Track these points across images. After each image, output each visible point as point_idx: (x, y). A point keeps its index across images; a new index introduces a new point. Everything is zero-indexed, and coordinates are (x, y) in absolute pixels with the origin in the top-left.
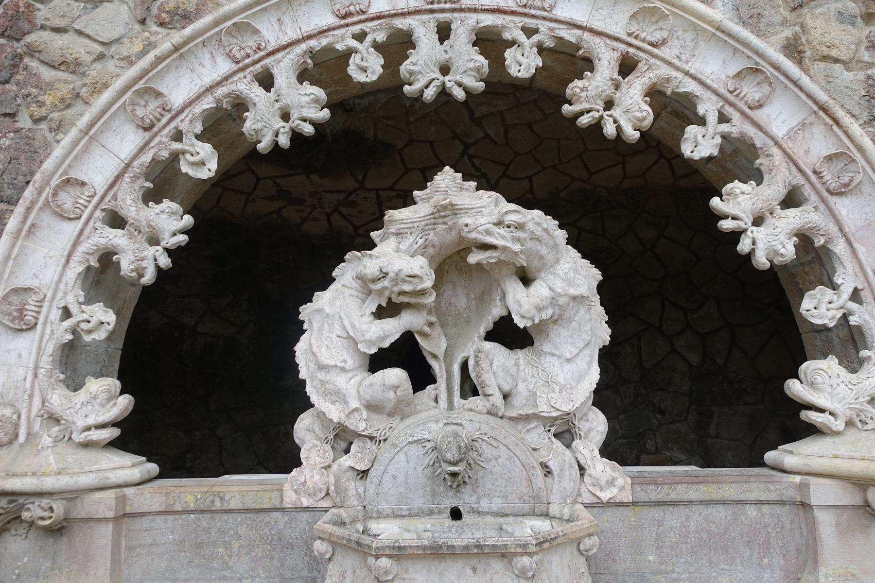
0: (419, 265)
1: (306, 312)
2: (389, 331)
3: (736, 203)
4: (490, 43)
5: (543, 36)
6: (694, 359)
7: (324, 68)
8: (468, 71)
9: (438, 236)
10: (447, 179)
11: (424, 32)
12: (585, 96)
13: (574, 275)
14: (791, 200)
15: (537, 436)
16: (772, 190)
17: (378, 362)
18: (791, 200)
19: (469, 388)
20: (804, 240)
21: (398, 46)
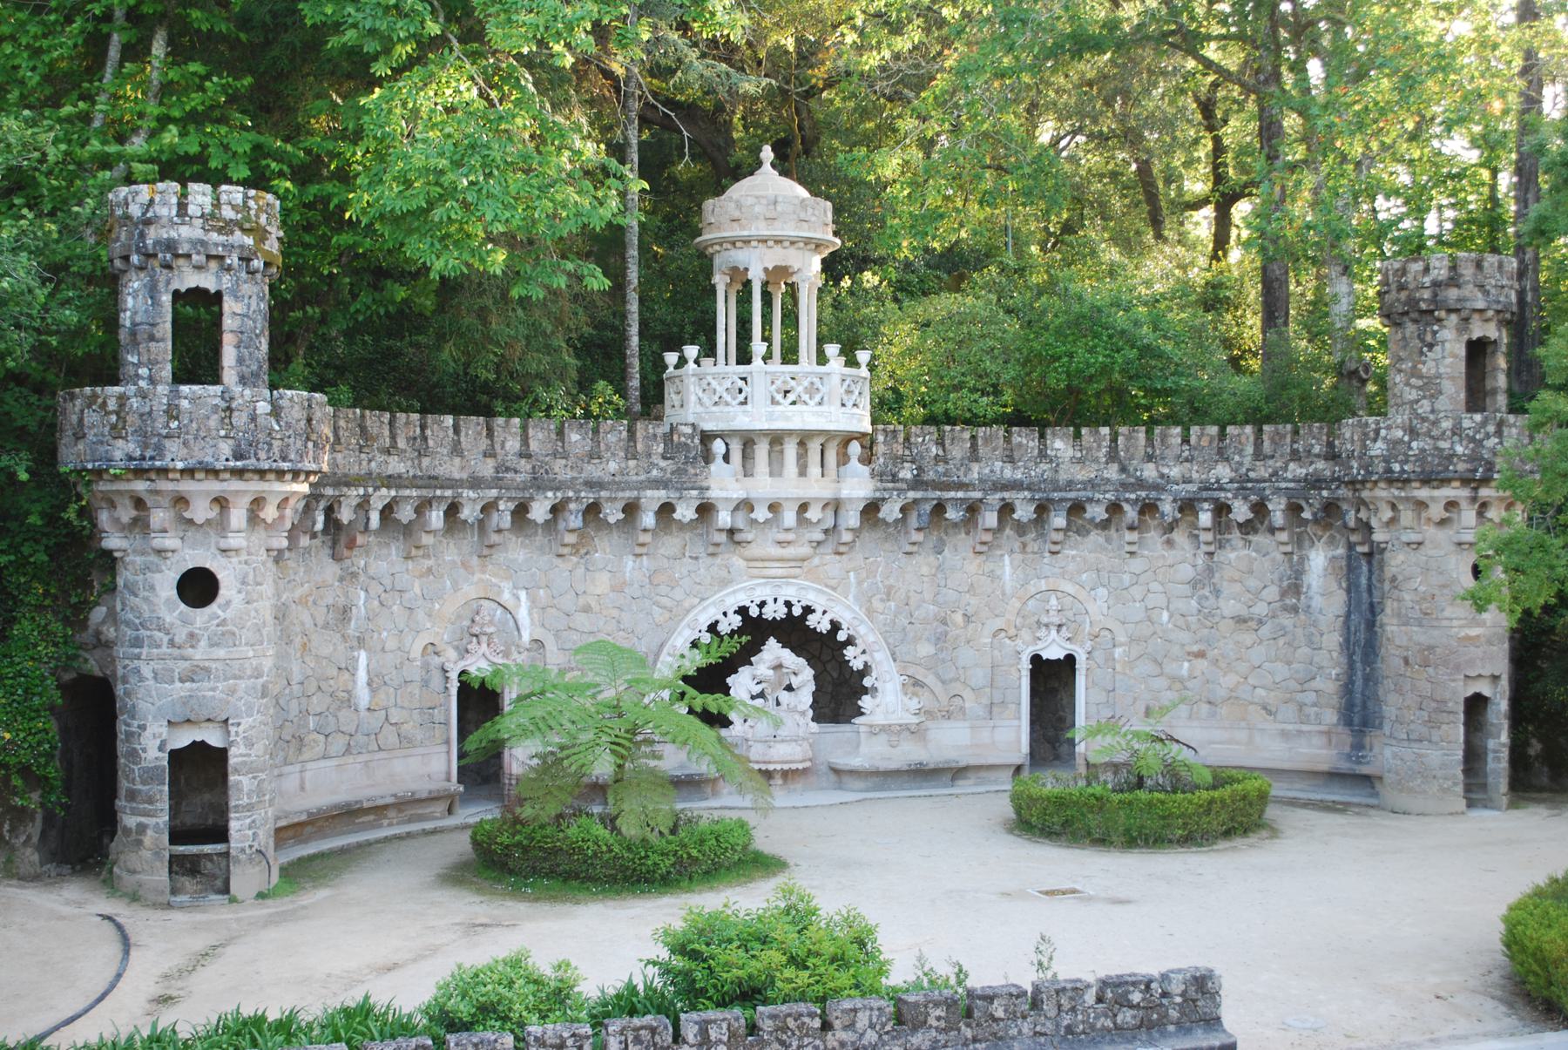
0: (771, 672)
1: (729, 680)
2: (758, 689)
3: (849, 652)
4: (788, 604)
5: (804, 603)
6: (835, 675)
7: (742, 611)
8: (781, 613)
9: (775, 663)
10: (772, 641)
11: (770, 601)
12: (812, 621)
13: (808, 673)
14: (864, 652)
15: (797, 716)
16: (859, 650)
17: (753, 698)
18: (864, 652)
19: (778, 704)
20: (866, 664)
21: (762, 604)
